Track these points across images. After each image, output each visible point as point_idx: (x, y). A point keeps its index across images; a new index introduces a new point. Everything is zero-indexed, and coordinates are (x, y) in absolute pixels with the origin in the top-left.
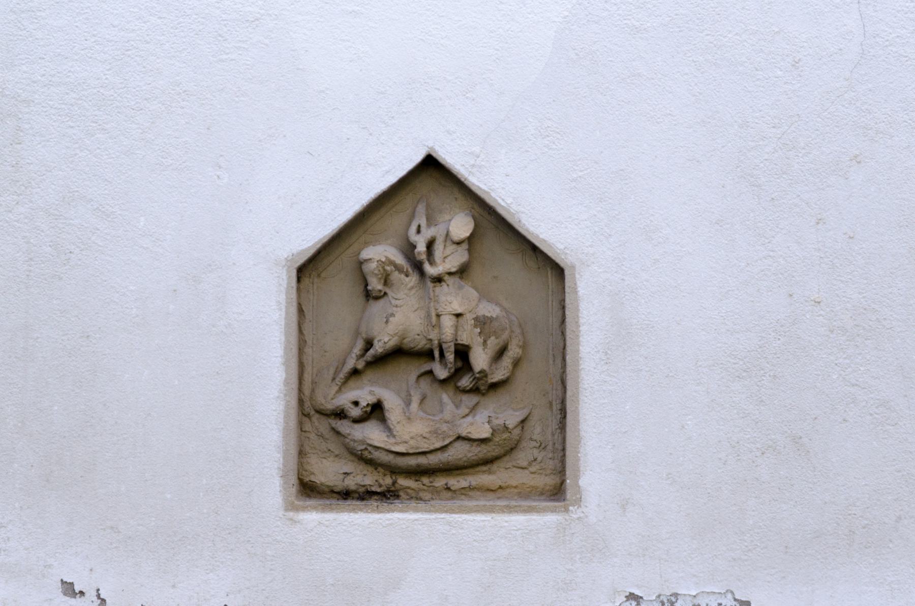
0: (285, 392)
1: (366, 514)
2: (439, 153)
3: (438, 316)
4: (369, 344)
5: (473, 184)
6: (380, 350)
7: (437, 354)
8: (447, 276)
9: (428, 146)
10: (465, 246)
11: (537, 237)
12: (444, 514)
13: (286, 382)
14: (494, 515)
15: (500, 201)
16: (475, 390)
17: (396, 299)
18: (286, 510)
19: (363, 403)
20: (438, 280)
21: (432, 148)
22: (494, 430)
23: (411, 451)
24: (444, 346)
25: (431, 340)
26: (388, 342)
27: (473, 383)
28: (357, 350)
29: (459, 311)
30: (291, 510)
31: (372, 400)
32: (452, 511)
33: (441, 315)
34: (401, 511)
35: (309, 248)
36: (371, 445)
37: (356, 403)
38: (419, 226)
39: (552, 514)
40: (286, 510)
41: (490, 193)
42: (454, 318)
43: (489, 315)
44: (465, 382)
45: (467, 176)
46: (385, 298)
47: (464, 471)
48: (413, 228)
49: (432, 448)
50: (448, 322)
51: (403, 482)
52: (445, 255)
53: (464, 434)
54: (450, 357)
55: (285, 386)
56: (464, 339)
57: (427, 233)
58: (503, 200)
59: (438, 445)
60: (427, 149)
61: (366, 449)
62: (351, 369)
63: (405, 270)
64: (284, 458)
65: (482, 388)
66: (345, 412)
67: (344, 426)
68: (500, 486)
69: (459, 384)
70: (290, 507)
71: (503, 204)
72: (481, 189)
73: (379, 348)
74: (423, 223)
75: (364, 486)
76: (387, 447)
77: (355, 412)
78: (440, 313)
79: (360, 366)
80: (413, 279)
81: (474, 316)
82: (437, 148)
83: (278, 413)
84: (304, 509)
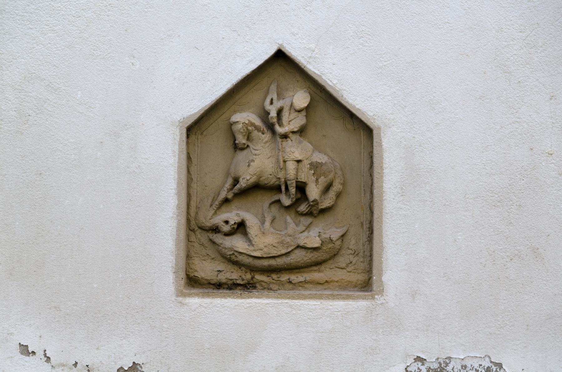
0: (177, 214)
1: (233, 299)
2: (287, 49)
3: (285, 162)
4: (236, 181)
5: (310, 70)
6: (244, 185)
7: (283, 188)
8: (291, 134)
9: (278, 44)
10: (304, 113)
11: (354, 107)
12: (287, 300)
13: (178, 207)
14: (322, 301)
15: (329, 82)
16: (309, 214)
17: (256, 150)
18: (177, 296)
19: (232, 222)
20: (285, 136)
21: (281, 45)
22: (323, 242)
23: (265, 256)
24: (289, 183)
25: (279, 178)
26: (249, 180)
27: (308, 209)
28: (228, 185)
29: (300, 158)
30: (180, 296)
31: (237, 219)
32: (293, 298)
33: (287, 161)
34: (257, 297)
35: (195, 114)
36: (236, 251)
37: (227, 222)
38: (272, 99)
39: (363, 300)
40: (177, 296)
41: (321, 76)
42: (295, 163)
43: (320, 161)
44: (303, 208)
45: (305, 64)
46: (248, 149)
47: (302, 270)
48: (268, 101)
49: (279, 253)
50: (291, 166)
51: (259, 277)
52: (290, 120)
53: (302, 244)
54: (293, 190)
55: (177, 209)
56: (303, 178)
57: (278, 104)
58: (331, 81)
59: (284, 251)
60: (278, 46)
61: (233, 254)
62: (224, 198)
63: (262, 130)
64: (176, 260)
65: (315, 212)
66: (219, 228)
67: (218, 238)
68: (326, 281)
69: (299, 209)
70: (180, 294)
71: (330, 84)
72: (315, 73)
73: (243, 184)
74: (275, 97)
75: (231, 280)
76: (248, 253)
77: (226, 228)
78: (286, 160)
79: (230, 196)
80: (267, 136)
81: (310, 162)
82: (285, 45)
83: (173, 228)
84: (190, 295)
